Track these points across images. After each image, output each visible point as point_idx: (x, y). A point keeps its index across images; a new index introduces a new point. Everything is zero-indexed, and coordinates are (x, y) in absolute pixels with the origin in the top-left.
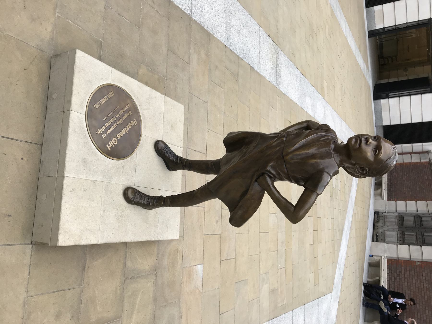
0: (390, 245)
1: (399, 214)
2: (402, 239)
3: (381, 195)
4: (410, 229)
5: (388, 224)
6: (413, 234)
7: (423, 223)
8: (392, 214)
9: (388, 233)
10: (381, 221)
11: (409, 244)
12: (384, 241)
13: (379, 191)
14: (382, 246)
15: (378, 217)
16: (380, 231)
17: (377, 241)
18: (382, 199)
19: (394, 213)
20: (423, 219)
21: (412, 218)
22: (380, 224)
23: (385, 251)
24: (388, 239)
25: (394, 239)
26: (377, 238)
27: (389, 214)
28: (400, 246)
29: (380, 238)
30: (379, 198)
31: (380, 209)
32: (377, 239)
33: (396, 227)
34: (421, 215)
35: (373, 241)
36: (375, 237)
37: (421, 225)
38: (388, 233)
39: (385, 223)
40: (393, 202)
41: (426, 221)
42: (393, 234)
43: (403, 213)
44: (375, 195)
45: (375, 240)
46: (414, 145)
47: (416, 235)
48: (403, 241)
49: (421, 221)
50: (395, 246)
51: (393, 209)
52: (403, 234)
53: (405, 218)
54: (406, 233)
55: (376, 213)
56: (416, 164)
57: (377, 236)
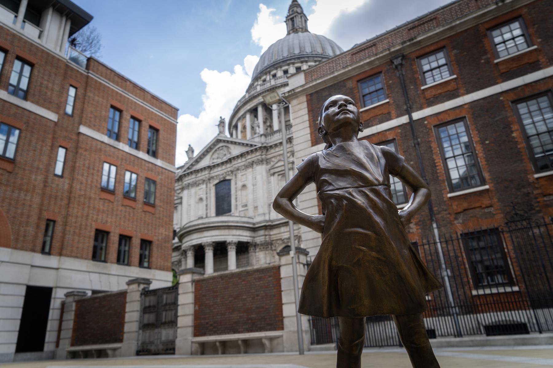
0: (178, 335)
1: (140, 329)
3: (114, 350)
4: (158, 316)
5: (152, 339)
6: (164, 313)
7: (152, 304)
8: (140, 336)
10: (149, 347)
11: (176, 316)
12: (173, 342)
13: (110, 352)
14: (179, 343)
15: (143, 351)
16: (161, 347)
17: (174, 349)
19: (139, 334)
20: (147, 304)
21: (146, 316)
22: (153, 348)
24: (171, 338)
25: (170, 331)
26: (169, 349)
28: (179, 325)
29: (171, 347)
30: (118, 352)
31: (134, 349)
32: (170, 350)
33: (156, 330)
34: (143, 307)
35: (174, 354)
37: (154, 307)
39: (151, 343)
40: (125, 336)
41: (150, 302)
42: (165, 333)
43: (139, 325)
44: (114, 356)
45: (172, 352)
46: (50, 317)
47: (166, 311)
48: (173, 323)
49: (150, 307)
50: (179, 331)
51: (135, 335)
52: (165, 323)
53: (146, 321)
54: (164, 320)
56: (76, 315)
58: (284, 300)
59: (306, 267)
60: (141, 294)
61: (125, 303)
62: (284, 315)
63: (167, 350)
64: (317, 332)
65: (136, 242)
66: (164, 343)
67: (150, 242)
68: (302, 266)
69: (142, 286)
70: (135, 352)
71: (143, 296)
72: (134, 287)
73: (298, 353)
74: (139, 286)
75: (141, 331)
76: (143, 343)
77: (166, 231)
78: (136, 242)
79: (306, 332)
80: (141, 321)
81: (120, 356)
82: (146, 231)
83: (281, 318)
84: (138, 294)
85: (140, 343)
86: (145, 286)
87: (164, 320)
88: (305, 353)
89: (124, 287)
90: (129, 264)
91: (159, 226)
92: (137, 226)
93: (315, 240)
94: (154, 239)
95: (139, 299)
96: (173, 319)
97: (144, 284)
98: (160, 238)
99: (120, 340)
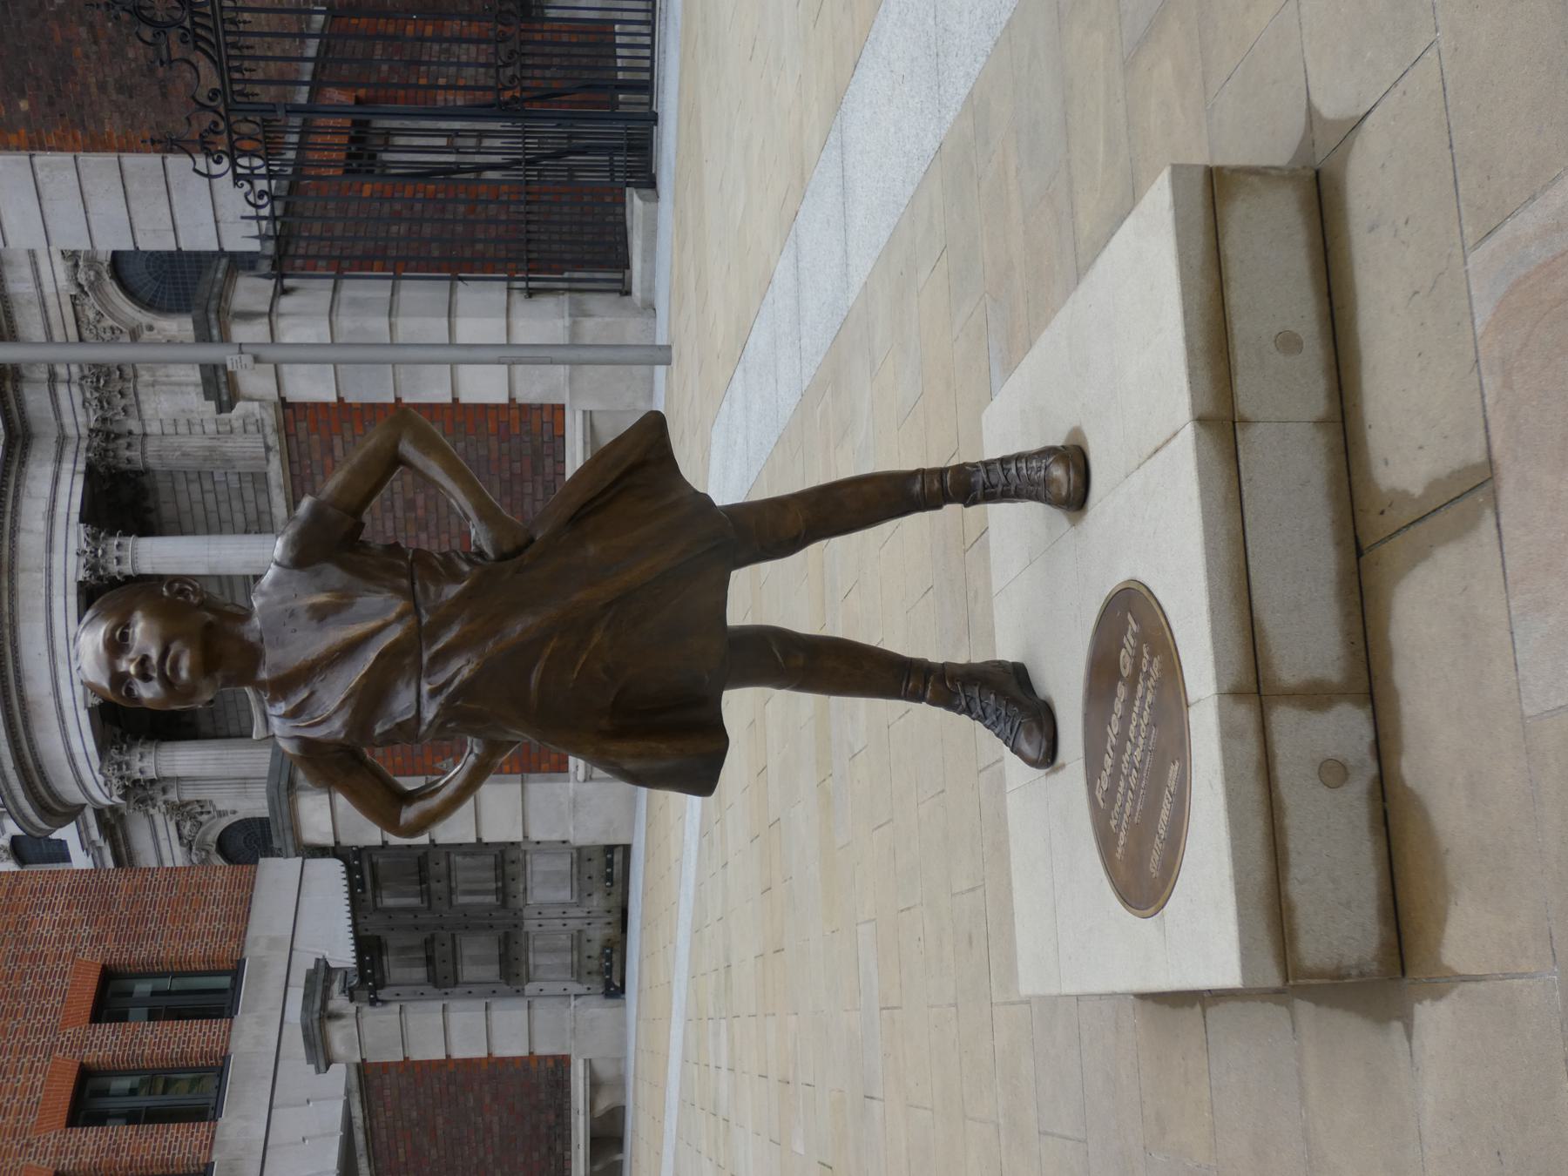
0: (556, 837)
1: (519, 993)
2: (509, 869)
3: (595, 1085)
4: (472, 923)
5: (564, 940)
6: (462, 900)
8: (549, 988)
9: (564, 895)
10: (595, 949)
11: (480, 847)
12: (581, 855)
13: (603, 1104)
14: (590, 832)
15: (609, 970)
16: (597, 902)
17: (610, 849)
18: (589, 1063)
20: (420, 973)
21: (469, 972)
22: (598, 933)
23: (575, 805)
24: (564, 864)
26: (608, 868)
27: (557, 988)
28: (517, 837)
30: (605, 1070)
31: (597, 1010)
32: (610, 863)
33: (530, 925)
34: (429, 989)
35: (627, 849)
36: (617, 868)
38: (564, 895)
40: (543, 1049)
42: (546, 888)
43: (505, 995)
44: (620, 1083)
45: (618, 857)
47: (451, 891)
48: (505, 860)
49: (429, 961)
51: (545, 1012)
52: (504, 894)
53: (492, 972)
54: (491, 899)
55: (614, 989)
57: (609, 878)
58: (439, 394)
59: (288, 282)
60: (373, 1002)
61: (408, 1066)
62: (504, 400)
63: (609, 878)
64: (579, 265)
65: (106, 1044)
66: (583, 894)
67: (109, 977)
68: (286, 303)
69: (339, 1002)
70: (611, 1002)
71: (382, 994)
72: (340, 1037)
73: (660, 370)
74: (336, 1016)
75: (530, 988)
76: (578, 974)
77: (51, 907)
78: (106, 1044)
79: (578, 313)
80: (489, 992)
81: (620, 1060)
82: (54, 1001)
83: (515, 413)
84: (371, 1015)
85: (575, 988)
86: (336, 987)
87: (491, 899)
88: (661, 340)
89: (338, 1076)
90: (216, 1069)
91: (23, 941)
92: (24, 1050)
93: (133, 187)
94: (93, 958)
95: (395, 1007)
96: (491, 860)
97: (326, 997)
98: (86, 931)
99: (561, 1064)
